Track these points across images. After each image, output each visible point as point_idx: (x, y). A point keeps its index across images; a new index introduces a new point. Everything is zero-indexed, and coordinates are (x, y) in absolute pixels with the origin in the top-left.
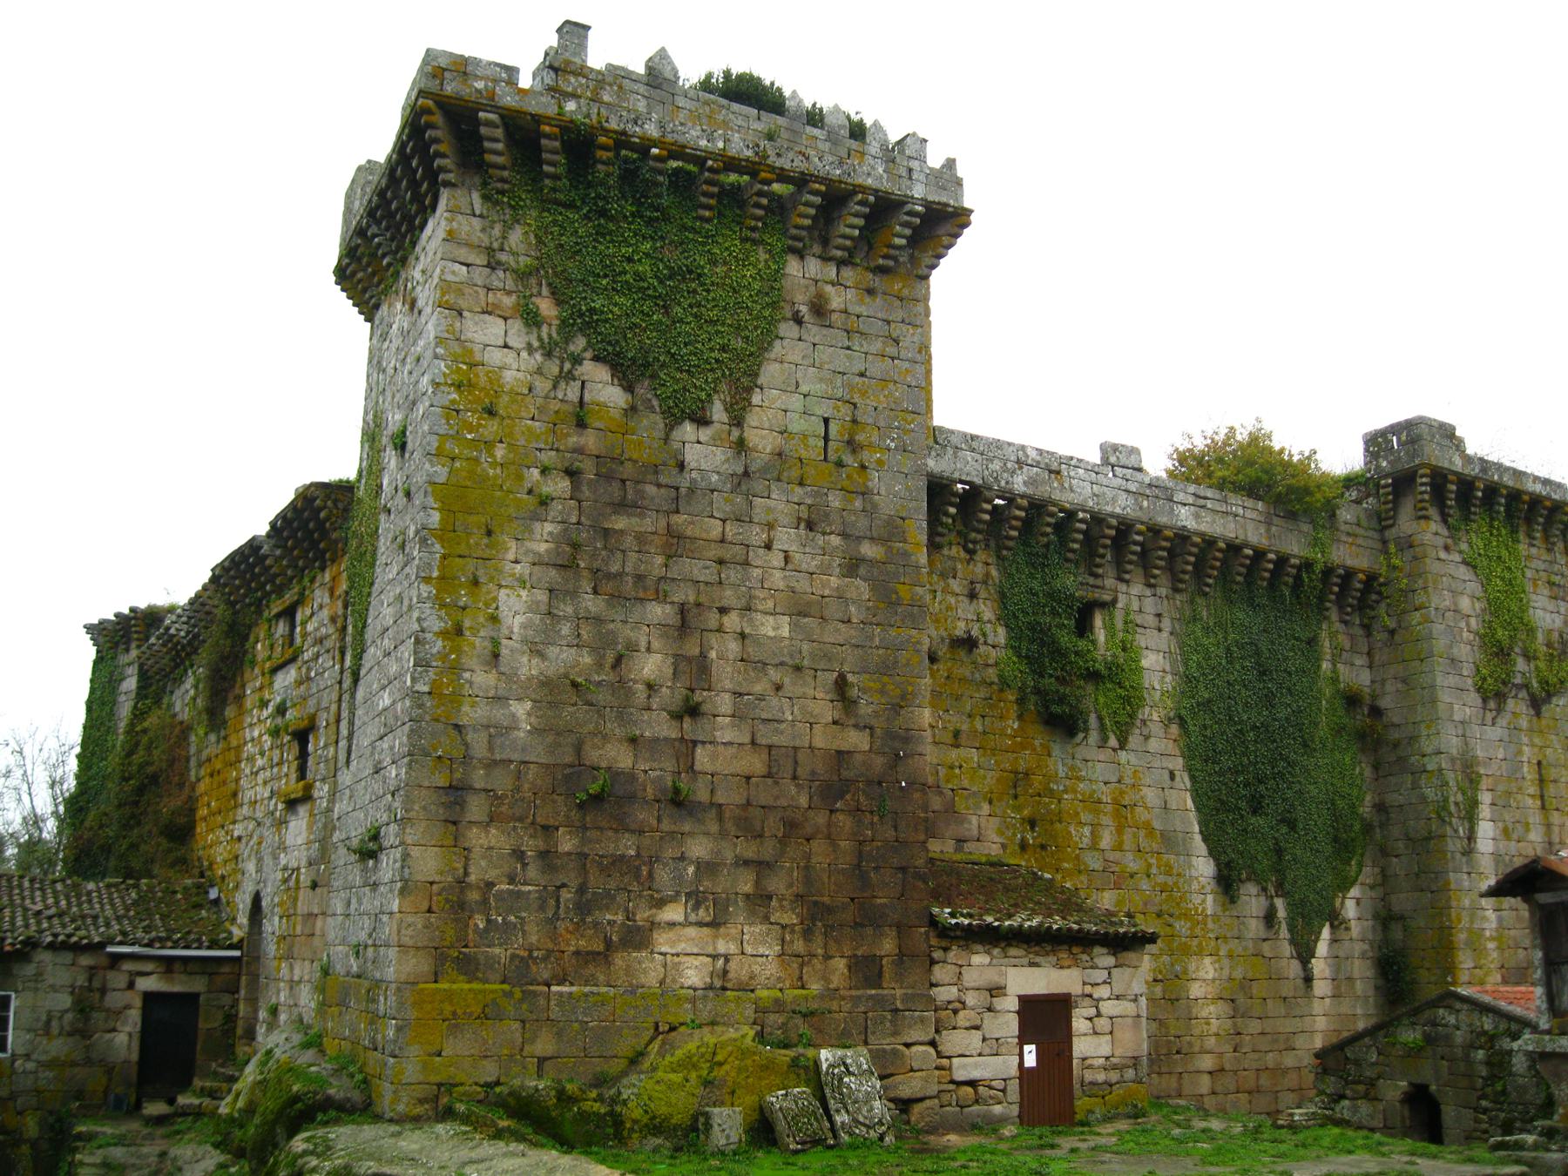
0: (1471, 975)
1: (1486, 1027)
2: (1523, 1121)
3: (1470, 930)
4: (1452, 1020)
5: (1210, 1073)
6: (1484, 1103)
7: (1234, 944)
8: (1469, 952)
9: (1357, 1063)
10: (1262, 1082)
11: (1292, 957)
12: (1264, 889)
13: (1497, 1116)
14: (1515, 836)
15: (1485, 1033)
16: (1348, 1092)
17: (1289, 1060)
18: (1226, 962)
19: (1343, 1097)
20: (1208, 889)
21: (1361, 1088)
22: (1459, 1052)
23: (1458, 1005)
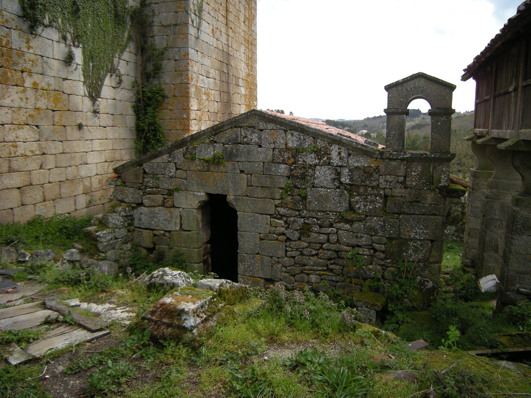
0: (196, 114)
1: (290, 145)
2: (321, 226)
3: (196, 87)
4: (255, 138)
5: (19, 188)
6: (282, 210)
7: (37, 78)
8: (196, 100)
9: (155, 176)
10: (63, 190)
11: (85, 96)
12: (65, 38)
13: (295, 221)
14: (216, 37)
15: (287, 149)
16: (146, 201)
17: (84, 172)
18: (30, 93)
19: (141, 204)
20: (13, 24)
21: (159, 198)
22: (259, 167)
23: (262, 125)
